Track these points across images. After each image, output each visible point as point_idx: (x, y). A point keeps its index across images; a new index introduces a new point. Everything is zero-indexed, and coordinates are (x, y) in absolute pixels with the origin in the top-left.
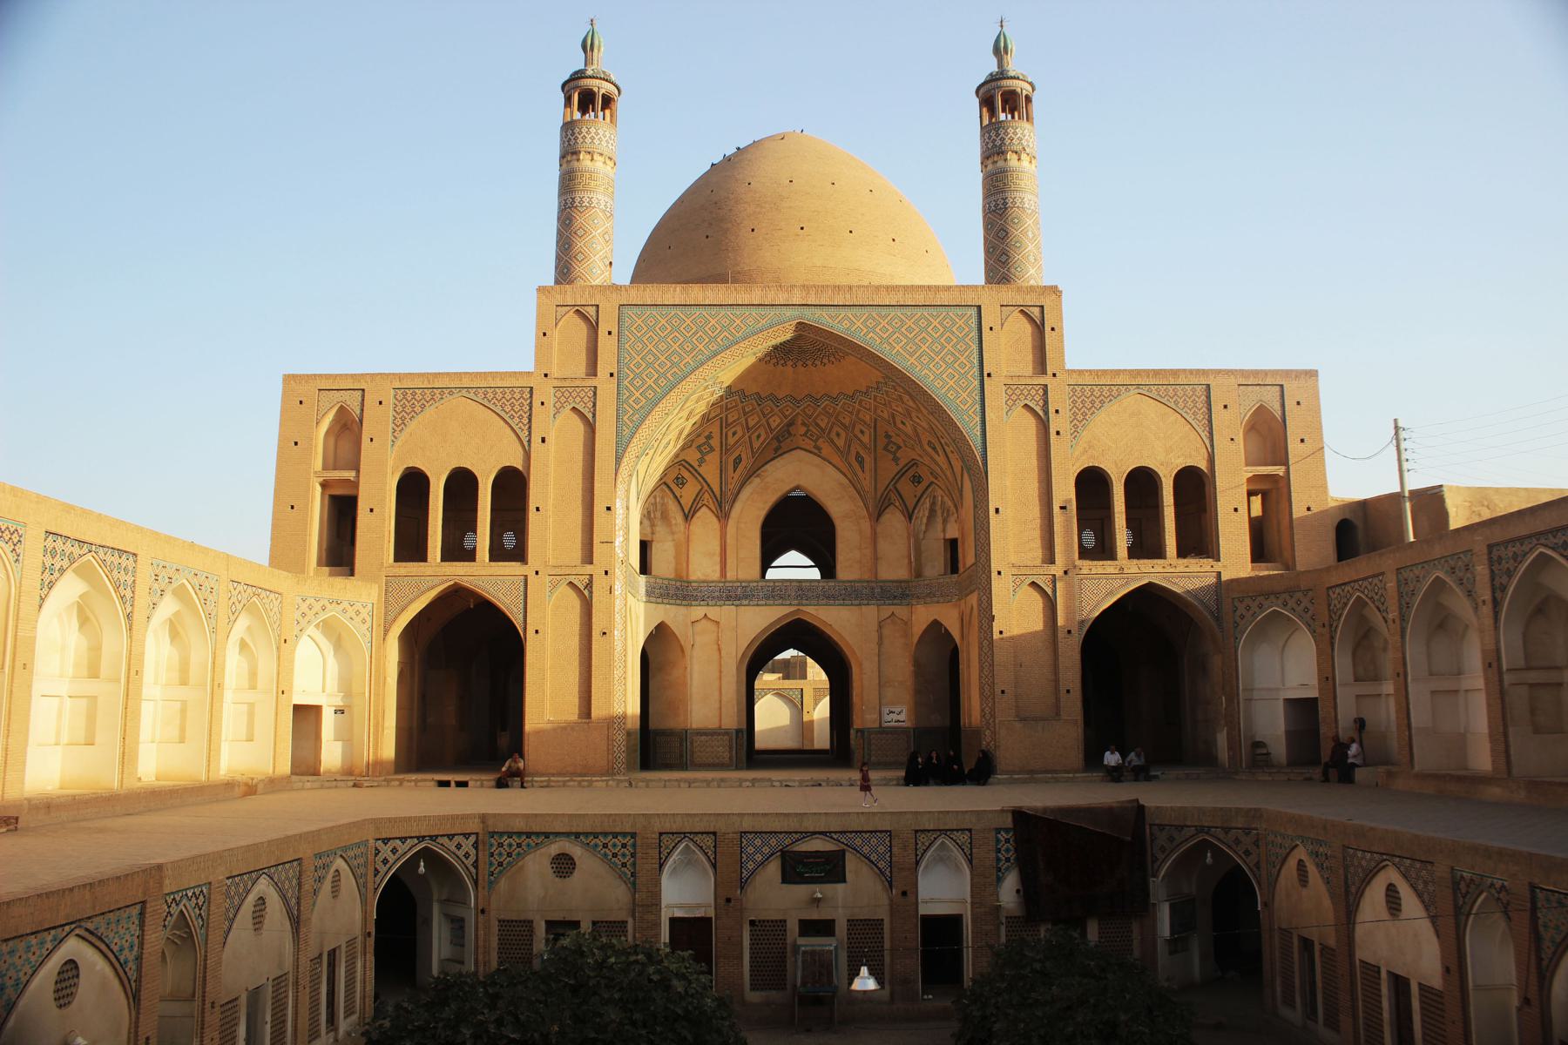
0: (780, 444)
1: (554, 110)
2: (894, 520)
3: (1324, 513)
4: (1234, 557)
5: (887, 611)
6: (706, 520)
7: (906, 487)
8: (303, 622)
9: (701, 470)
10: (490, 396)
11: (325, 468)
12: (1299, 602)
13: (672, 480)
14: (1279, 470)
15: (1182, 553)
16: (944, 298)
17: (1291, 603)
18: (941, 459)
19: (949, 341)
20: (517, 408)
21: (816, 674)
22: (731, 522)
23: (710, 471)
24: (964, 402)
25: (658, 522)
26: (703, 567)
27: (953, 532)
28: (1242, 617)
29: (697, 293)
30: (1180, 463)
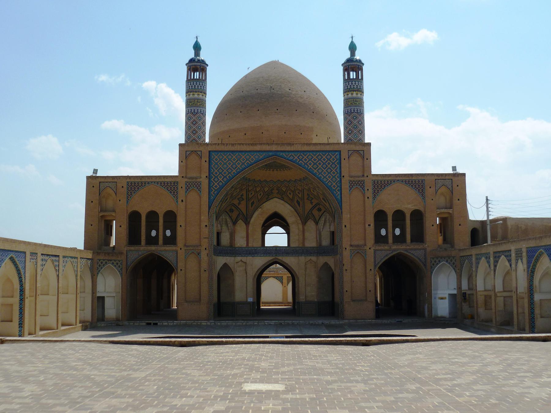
0: (268, 197)
2: (311, 224)
5: (309, 258)
6: (241, 225)
7: (315, 213)
8: (100, 268)
9: (239, 207)
10: (163, 185)
12: (451, 261)
16: (327, 148)
17: (449, 261)
18: (327, 205)
19: (329, 164)
20: (173, 189)
21: (286, 275)
23: (242, 207)
24: (334, 186)
25: (224, 225)
26: (240, 242)
27: (332, 229)
28: (433, 264)
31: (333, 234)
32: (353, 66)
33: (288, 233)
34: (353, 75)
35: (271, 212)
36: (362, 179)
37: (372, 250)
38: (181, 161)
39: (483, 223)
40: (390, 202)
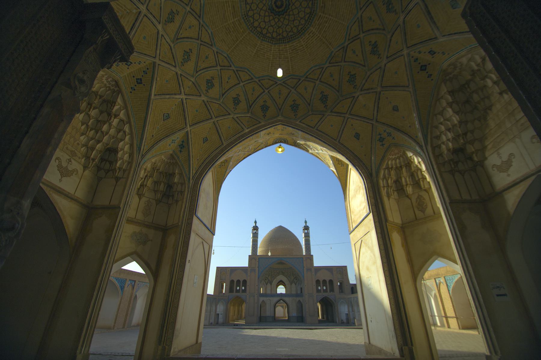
2: (293, 285)
7: (295, 280)
15: (330, 292)
26: (269, 292)
31: (301, 288)
32: (306, 228)
34: (306, 231)
38: (249, 261)
40: (321, 277)
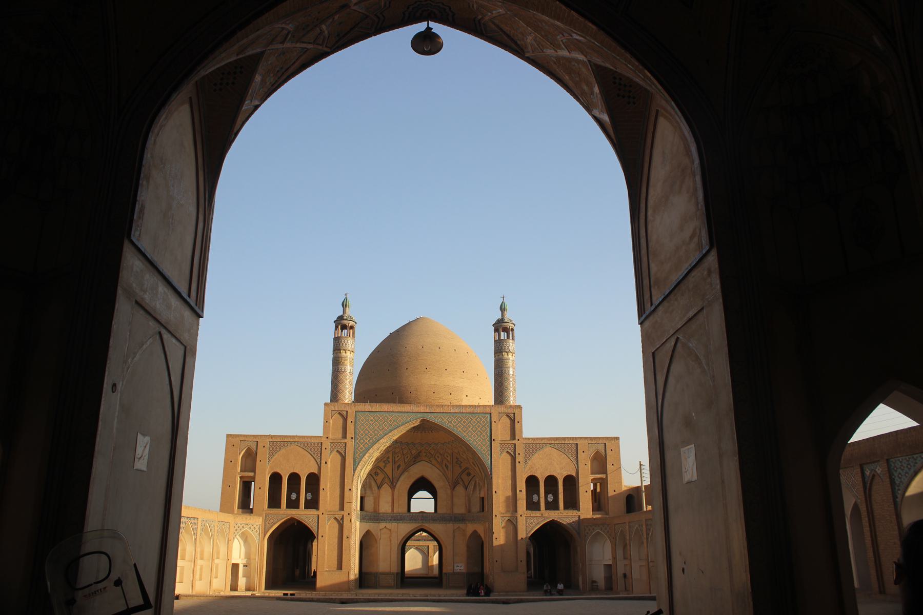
0: (416, 459)
1: (330, 332)
2: (460, 489)
3: (621, 493)
4: (586, 509)
5: (457, 525)
6: (386, 491)
7: (464, 477)
11: (241, 471)
13: (372, 475)
14: (603, 476)
15: (566, 508)
16: (478, 410)
18: (477, 469)
21: (433, 545)
22: (396, 490)
23: (388, 470)
26: (385, 507)
29: (385, 407)
30: (565, 474)
33: (435, 497)
34: (503, 335)
35: (418, 476)
36: (514, 442)
37: (524, 518)
39: (637, 489)
